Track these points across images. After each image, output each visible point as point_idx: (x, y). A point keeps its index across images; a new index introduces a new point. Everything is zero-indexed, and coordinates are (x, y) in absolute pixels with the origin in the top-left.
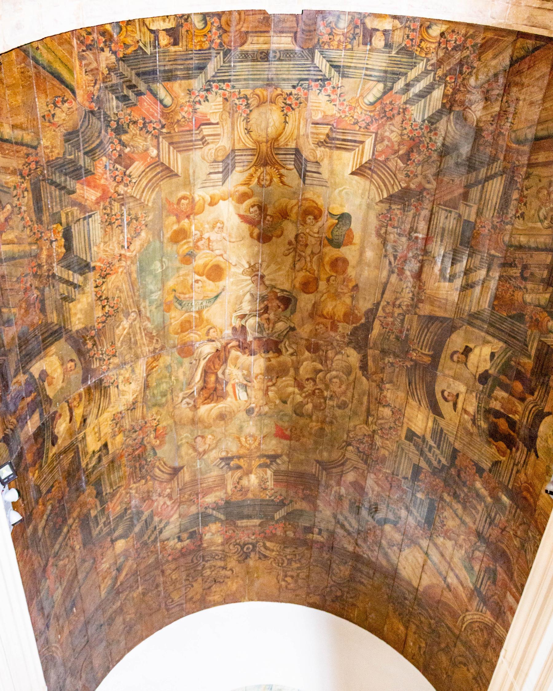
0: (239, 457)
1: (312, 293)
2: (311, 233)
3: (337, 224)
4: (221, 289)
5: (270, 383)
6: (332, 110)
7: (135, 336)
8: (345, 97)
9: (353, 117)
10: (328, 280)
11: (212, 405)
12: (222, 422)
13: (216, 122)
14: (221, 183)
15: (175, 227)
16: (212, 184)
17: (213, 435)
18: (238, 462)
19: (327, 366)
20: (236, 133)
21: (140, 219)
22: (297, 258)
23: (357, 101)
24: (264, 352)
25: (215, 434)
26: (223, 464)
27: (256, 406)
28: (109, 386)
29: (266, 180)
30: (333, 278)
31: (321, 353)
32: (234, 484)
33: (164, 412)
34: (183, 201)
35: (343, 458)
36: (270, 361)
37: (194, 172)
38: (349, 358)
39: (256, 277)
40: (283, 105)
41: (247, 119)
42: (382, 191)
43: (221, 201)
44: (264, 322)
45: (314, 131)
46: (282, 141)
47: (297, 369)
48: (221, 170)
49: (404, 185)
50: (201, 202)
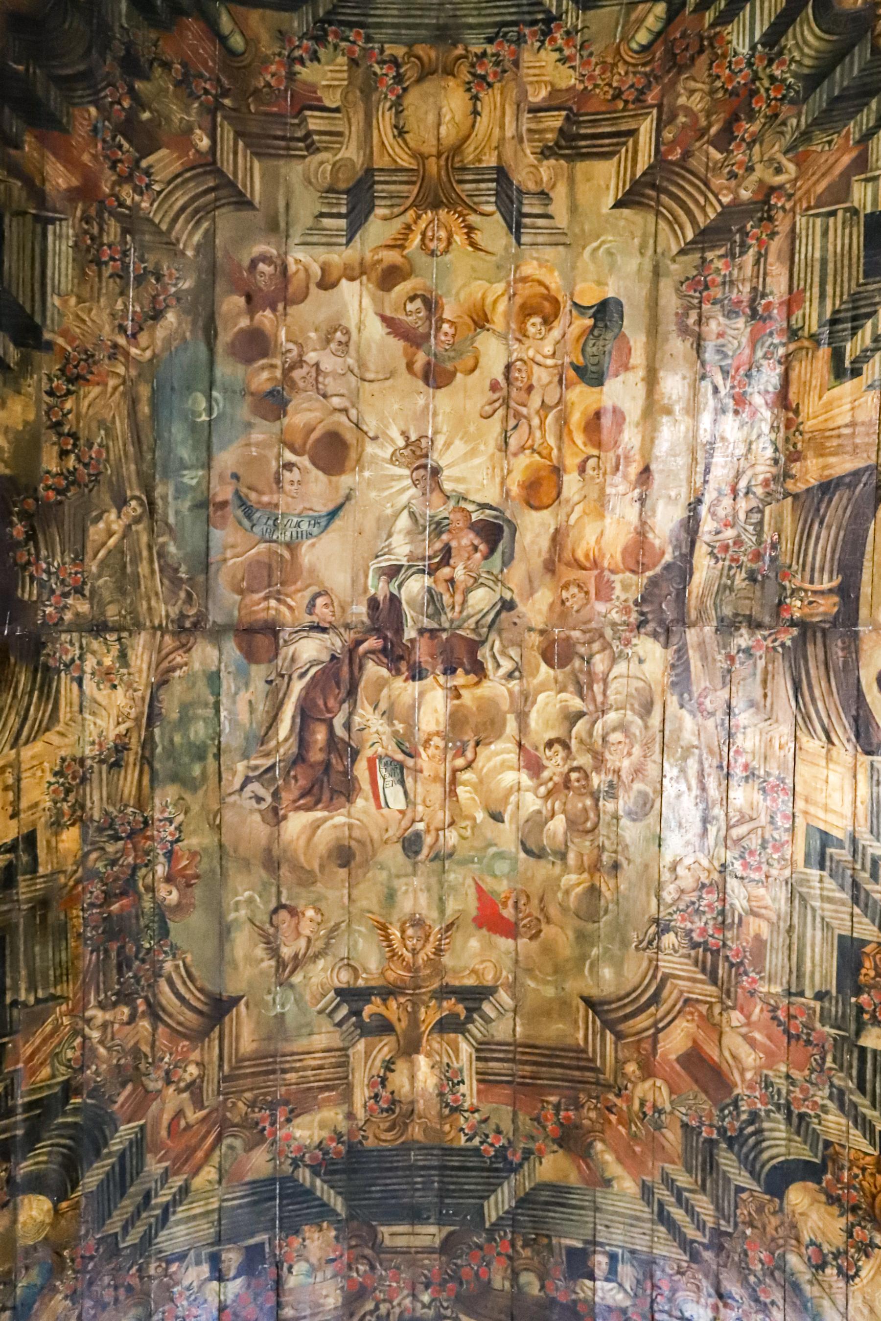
0: (388, 992)
1: (547, 507)
2: (539, 358)
3: (595, 326)
4: (343, 492)
5: (460, 762)
6: (567, 78)
7: (136, 559)
8: (592, 49)
9: (610, 85)
10: (582, 469)
11: (319, 814)
12: (343, 872)
13: (334, 106)
14: (344, 240)
15: (244, 322)
16: (324, 240)
17: (318, 910)
18: (382, 1010)
19: (594, 700)
20: (375, 133)
21: (166, 279)
22: (512, 422)
23: (618, 51)
24: (445, 673)
25: (323, 906)
26: (344, 1011)
27: (428, 831)
28: (59, 672)
29: (439, 239)
30: (592, 462)
31: (577, 663)
32: (371, 1085)
33: (195, 802)
34: (262, 266)
35: (654, 976)
36: (459, 696)
37: (287, 206)
38: (645, 667)
39: (422, 472)
40: (469, 78)
41: (398, 106)
42: (682, 228)
43: (344, 282)
44: (441, 588)
45: (533, 126)
46: (469, 154)
47: (522, 717)
48: (344, 210)
49: (726, 200)
50: (302, 275)
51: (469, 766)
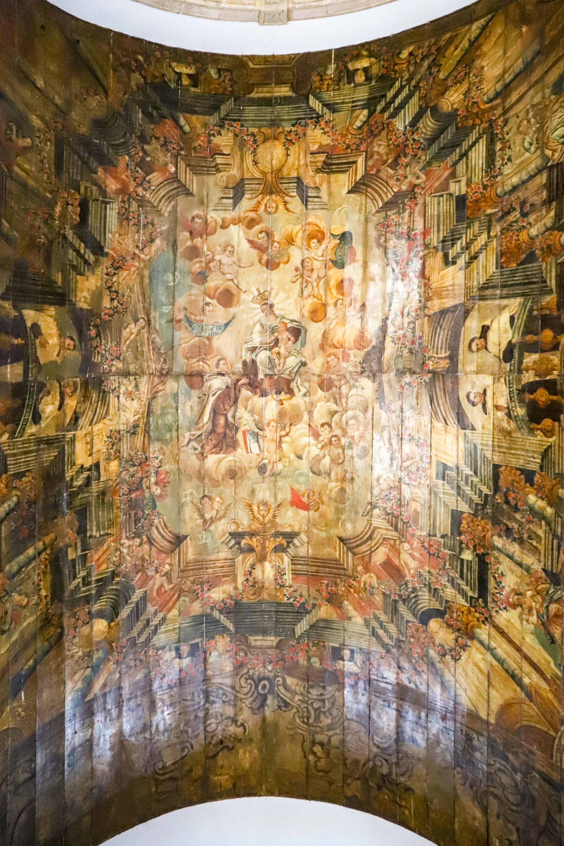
5: (283, 433)
36: (282, 404)
50: (213, 223)
51: (287, 434)
